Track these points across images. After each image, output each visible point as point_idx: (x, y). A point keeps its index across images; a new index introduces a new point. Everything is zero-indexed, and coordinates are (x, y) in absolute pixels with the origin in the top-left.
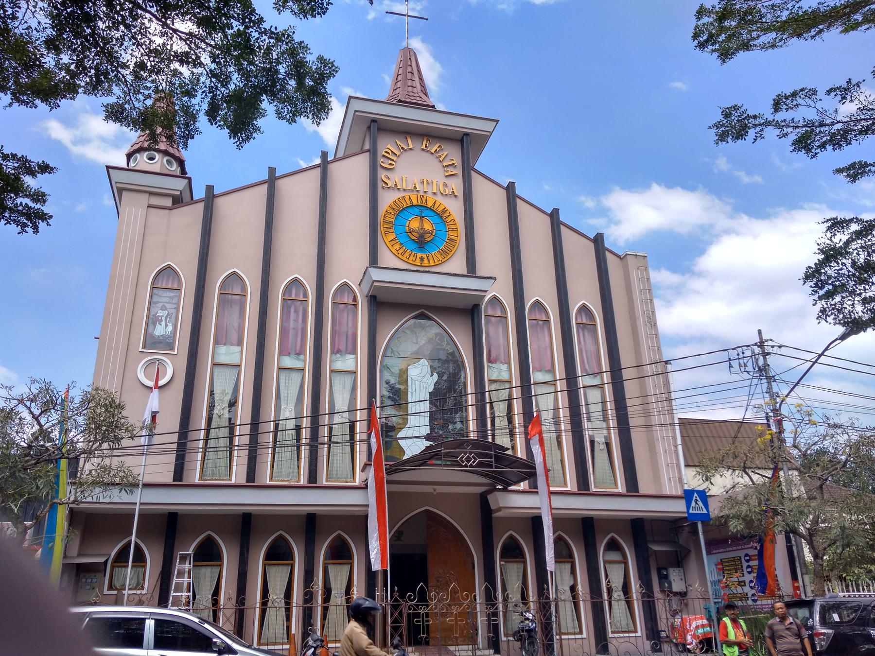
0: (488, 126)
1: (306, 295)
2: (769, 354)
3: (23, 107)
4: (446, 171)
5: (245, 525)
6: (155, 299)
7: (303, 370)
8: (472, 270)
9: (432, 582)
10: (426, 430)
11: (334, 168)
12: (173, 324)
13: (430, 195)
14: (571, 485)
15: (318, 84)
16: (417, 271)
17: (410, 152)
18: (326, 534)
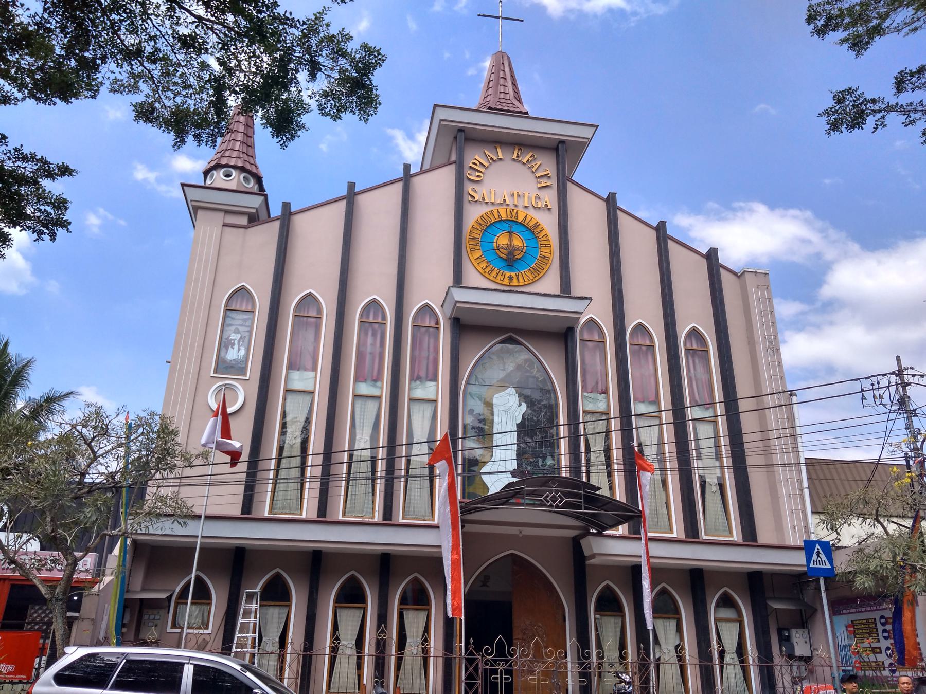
0: (586, 133)
1: (384, 317)
2: (909, 384)
3: (41, 105)
4: (539, 182)
5: (315, 564)
6: (228, 321)
7: (379, 398)
8: (566, 290)
9: (517, 635)
10: (513, 465)
11: (417, 182)
12: (246, 348)
13: (520, 208)
14: (678, 532)
15: (363, 75)
16: (504, 291)
17: (500, 163)
18: (397, 576)
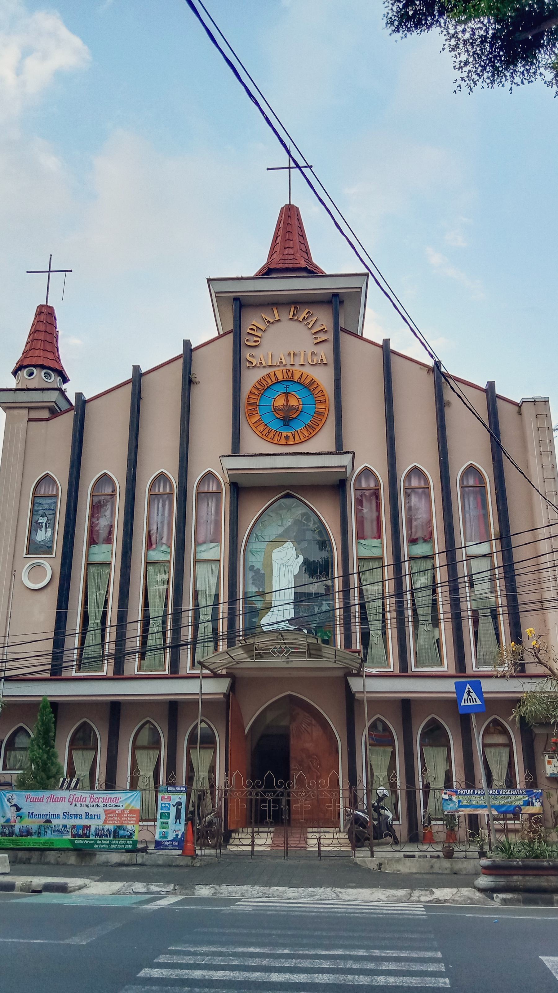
4: (316, 338)
13: (297, 368)
17: (278, 324)
